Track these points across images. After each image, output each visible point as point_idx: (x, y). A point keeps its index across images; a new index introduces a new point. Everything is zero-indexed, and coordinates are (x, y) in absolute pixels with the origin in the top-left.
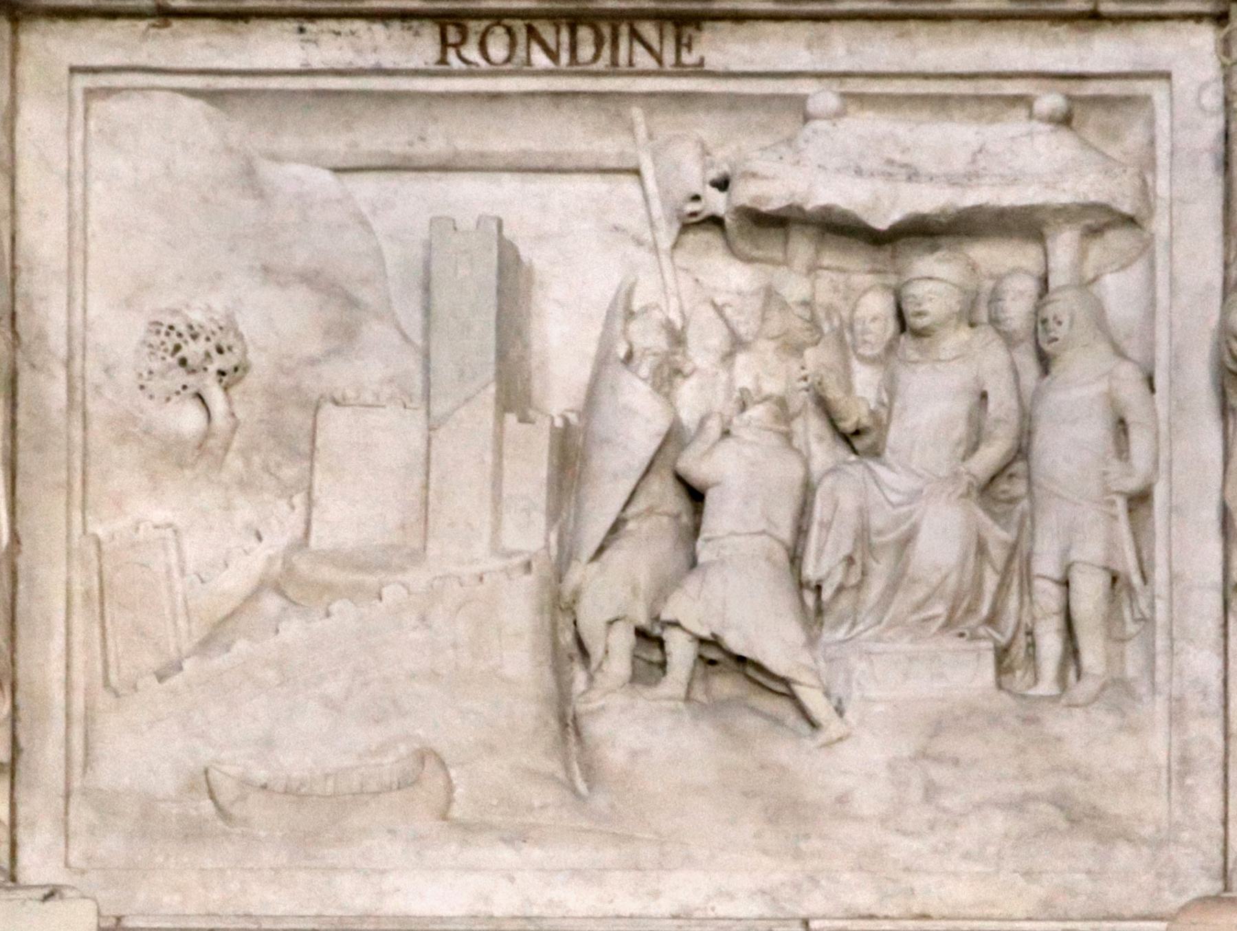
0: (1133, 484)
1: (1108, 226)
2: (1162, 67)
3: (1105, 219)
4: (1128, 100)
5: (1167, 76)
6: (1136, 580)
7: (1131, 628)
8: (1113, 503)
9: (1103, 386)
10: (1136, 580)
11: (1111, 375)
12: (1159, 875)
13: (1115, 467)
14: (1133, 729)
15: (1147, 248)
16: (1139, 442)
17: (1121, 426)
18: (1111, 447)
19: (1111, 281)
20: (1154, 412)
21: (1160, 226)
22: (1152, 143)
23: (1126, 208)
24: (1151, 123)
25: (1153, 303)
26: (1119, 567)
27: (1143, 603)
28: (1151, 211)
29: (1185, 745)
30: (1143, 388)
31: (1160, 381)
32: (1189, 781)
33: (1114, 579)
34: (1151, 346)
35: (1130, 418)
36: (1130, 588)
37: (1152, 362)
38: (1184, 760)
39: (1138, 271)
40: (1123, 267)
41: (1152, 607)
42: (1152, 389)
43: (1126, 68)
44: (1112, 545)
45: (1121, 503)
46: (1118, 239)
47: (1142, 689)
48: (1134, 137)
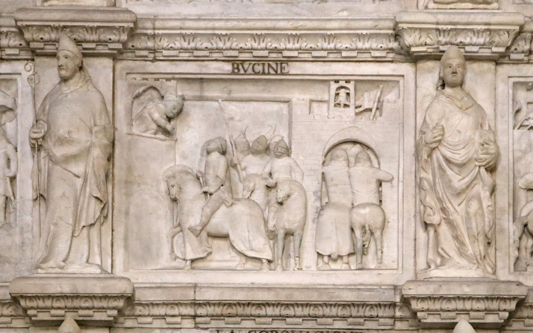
0: (11, 175)
1: (7, 111)
2: (19, 72)
3: (5, 109)
4: (11, 80)
5: (20, 74)
6: (12, 198)
7: (12, 210)
8: (6, 179)
9: (4, 150)
10: (12, 198)
11: (6, 147)
12: (16, 271)
13: (7, 170)
14: (10, 235)
15: (16, 116)
16: (13, 165)
17: (9, 160)
18: (6, 166)
19: (8, 124)
20: (17, 157)
21: (19, 111)
22: (17, 90)
23: (10, 106)
24: (17, 85)
25: (17, 130)
26: (8, 195)
27: (14, 204)
28: (16, 107)
29: (23, 238)
30: (14, 150)
31: (19, 149)
32: (24, 248)
33: (7, 198)
34: (17, 140)
35: (10, 158)
36: (11, 200)
37: (17, 144)
38: (23, 243)
39: (14, 121)
40: (11, 121)
41: (16, 205)
42: (17, 151)
43: (9, 72)
44: (6, 190)
45: (8, 179)
46: (9, 114)
47: (14, 225)
48: (13, 89)
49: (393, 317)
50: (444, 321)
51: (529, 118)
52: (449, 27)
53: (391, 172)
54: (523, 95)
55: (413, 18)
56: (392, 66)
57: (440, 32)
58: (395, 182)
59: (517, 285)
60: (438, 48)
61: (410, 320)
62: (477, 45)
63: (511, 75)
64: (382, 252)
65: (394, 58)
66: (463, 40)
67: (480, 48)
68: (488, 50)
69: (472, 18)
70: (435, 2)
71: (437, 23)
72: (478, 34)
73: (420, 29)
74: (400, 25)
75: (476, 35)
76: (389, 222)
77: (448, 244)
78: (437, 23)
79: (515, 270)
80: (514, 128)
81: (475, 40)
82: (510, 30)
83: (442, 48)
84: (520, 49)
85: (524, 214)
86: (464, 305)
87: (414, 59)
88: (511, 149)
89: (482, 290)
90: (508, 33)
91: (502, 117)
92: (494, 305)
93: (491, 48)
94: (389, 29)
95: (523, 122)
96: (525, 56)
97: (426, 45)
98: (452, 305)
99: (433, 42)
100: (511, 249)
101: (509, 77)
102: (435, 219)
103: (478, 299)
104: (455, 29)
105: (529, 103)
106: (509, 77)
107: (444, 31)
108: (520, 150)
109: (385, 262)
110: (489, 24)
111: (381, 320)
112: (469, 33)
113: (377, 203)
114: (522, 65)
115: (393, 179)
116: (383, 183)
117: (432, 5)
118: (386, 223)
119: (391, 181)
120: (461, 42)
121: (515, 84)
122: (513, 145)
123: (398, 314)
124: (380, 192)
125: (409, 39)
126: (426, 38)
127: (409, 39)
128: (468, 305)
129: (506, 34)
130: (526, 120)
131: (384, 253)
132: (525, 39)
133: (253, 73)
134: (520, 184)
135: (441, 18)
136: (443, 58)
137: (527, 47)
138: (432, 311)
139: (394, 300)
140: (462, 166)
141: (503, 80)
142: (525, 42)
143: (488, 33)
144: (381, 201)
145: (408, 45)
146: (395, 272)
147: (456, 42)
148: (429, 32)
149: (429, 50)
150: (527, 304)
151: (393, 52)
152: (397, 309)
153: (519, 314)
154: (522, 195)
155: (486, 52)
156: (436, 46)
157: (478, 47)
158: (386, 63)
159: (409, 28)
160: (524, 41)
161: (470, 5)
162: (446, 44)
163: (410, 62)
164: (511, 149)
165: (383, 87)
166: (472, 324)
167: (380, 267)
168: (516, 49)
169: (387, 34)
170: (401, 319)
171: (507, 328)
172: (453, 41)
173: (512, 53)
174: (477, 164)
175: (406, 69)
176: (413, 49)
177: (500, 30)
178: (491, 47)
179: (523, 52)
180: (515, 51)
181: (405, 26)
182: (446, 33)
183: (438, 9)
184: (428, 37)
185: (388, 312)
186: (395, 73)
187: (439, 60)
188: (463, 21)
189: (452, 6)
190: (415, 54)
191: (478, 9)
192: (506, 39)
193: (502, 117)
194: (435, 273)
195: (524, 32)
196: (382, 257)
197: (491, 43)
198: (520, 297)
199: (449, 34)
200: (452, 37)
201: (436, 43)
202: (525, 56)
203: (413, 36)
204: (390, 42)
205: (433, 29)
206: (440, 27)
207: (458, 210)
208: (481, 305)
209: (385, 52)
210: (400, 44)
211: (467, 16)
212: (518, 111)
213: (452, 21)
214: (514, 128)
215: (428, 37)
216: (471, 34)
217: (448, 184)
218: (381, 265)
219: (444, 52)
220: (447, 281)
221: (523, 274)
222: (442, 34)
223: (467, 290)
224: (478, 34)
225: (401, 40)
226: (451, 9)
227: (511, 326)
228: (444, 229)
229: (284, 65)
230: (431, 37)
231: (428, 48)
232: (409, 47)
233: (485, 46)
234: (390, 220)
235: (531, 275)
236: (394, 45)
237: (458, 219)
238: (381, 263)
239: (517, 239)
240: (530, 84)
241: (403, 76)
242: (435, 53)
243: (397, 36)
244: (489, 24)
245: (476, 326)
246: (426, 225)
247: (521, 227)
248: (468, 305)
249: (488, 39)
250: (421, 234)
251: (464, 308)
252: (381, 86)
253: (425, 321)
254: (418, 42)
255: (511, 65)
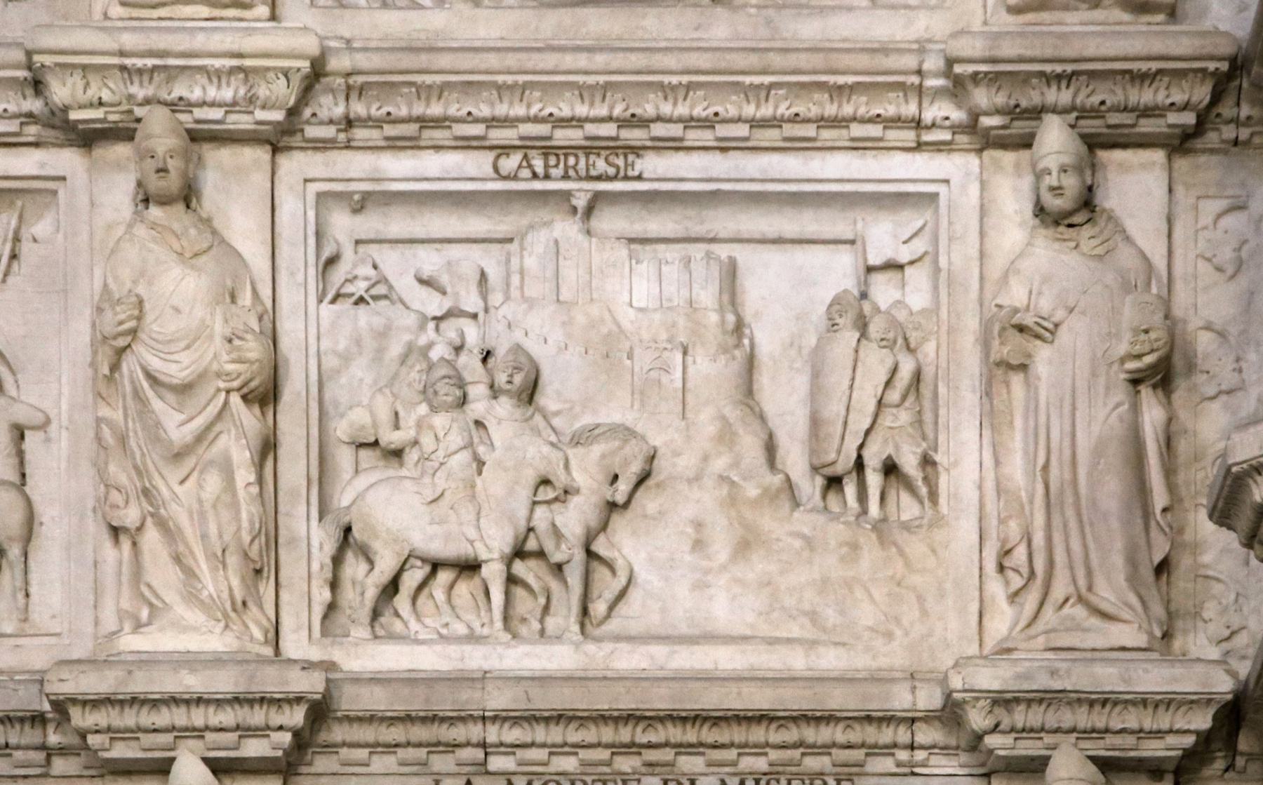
49: (43, 747)
50: (150, 755)
51: (356, 277)
52: (150, 62)
53: (42, 406)
54: (343, 225)
55: (64, 42)
56: (37, 155)
57: (130, 74)
58: (53, 427)
59: (304, 668)
60: (130, 112)
61: (83, 753)
62: (220, 106)
63: (310, 176)
64: (27, 595)
65: (39, 135)
66: (185, 94)
67: (227, 112)
68: (245, 118)
69: (199, 42)
70: (123, 4)
71: (122, 54)
72: (219, 78)
73: (85, 68)
74: (36, 58)
75: (215, 80)
76: (41, 524)
77: (162, 575)
78: (122, 54)
79: (325, 633)
80: (320, 301)
81: (212, 93)
82: (290, 68)
83: (139, 112)
84: (324, 114)
85: (345, 502)
86: (189, 717)
87: (87, 138)
88: (313, 350)
89: (224, 682)
90: (286, 76)
91: (292, 274)
92: (257, 716)
93: (252, 113)
94: (16, 66)
95: (343, 285)
96: (339, 131)
97: (101, 104)
98: (163, 717)
99: (116, 99)
100: (314, 583)
101: (306, 181)
102: (130, 516)
103: (219, 703)
104: (165, 67)
105: (357, 242)
106: (306, 181)
107: (140, 72)
108: (335, 352)
109: (34, 616)
110: (240, 56)
111: (18, 754)
112: (198, 76)
113: (15, 478)
114: (336, 152)
115: (48, 421)
116: (27, 433)
117: (117, 11)
118: (36, 526)
119: (44, 425)
120: (181, 99)
121: (320, 196)
122: (318, 338)
123: (54, 739)
124: (20, 454)
125: (61, 91)
126: (100, 89)
127: (61, 91)
128: (198, 717)
129: (283, 80)
130: (347, 280)
131: (34, 597)
132: (332, 91)
133: (496, 176)
134: (339, 433)
135: (129, 40)
136: (138, 135)
137: (339, 110)
138: (119, 731)
139: (38, 708)
140: (184, 389)
141: (291, 188)
142: (335, 98)
143: (242, 76)
144: (23, 475)
145: (61, 105)
146: (53, 640)
147: (168, 98)
148: (106, 73)
149: (112, 118)
150: (339, 714)
151: (36, 123)
152: (50, 729)
153: (323, 737)
154: (344, 458)
155: (240, 122)
156: (124, 107)
157: (223, 110)
158: (24, 149)
159: (57, 65)
160: (331, 97)
161: (205, 11)
162: (147, 102)
163: (79, 146)
164: (313, 350)
165: (23, 207)
166: (206, 761)
167: (23, 630)
168: (314, 115)
169: (14, 80)
170: (63, 751)
171: (304, 769)
172: (164, 96)
173: (308, 122)
174: (222, 385)
175: (67, 160)
176: (74, 115)
177: (268, 69)
178: (251, 108)
179: (331, 122)
180: (313, 120)
181: (48, 60)
182: (146, 78)
183: (131, 19)
184: (105, 85)
185: (31, 735)
186: (43, 173)
187: (131, 138)
188: (181, 48)
189: (162, 12)
190: (80, 127)
191: (222, 19)
192: (283, 91)
193: (292, 274)
194: (132, 642)
195: (326, 75)
196: (27, 605)
197: (251, 100)
198: (310, 696)
199: (151, 78)
200: (159, 86)
201: (124, 101)
202: (339, 131)
203: (70, 81)
204: (25, 98)
205: (114, 66)
206: (128, 62)
207: (182, 494)
208: (227, 717)
209: (18, 121)
210: (47, 104)
211: (188, 37)
212: (332, 261)
213: (154, 47)
214: (320, 301)
215: (105, 85)
216: (202, 79)
217: (154, 430)
218: (26, 626)
219: (138, 120)
220: (148, 661)
221: (342, 644)
222: (136, 79)
223: (192, 683)
224: (219, 78)
225: (47, 94)
226: (160, 19)
227: (310, 764)
228: (152, 538)
229: (592, 158)
230: (112, 85)
231: (106, 113)
232: (66, 109)
233: (237, 108)
234: (44, 520)
235: (357, 645)
236: (34, 105)
237: (180, 516)
238: (25, 620)
239: (328, 561)
240: (356, 197)
241: (947, 181)
242: (126, 125)
243: (37, 85)
244: (240, 56)
245: (217, 767)
246: (116, 531)
247: (338, 534)
248: (198, 717)
249: (242, 92)
250: (109, 552)
251: (189, 725)
252: (19, 203)
253: (106, 755)
254: (82, 98)
255: (310, 152)
